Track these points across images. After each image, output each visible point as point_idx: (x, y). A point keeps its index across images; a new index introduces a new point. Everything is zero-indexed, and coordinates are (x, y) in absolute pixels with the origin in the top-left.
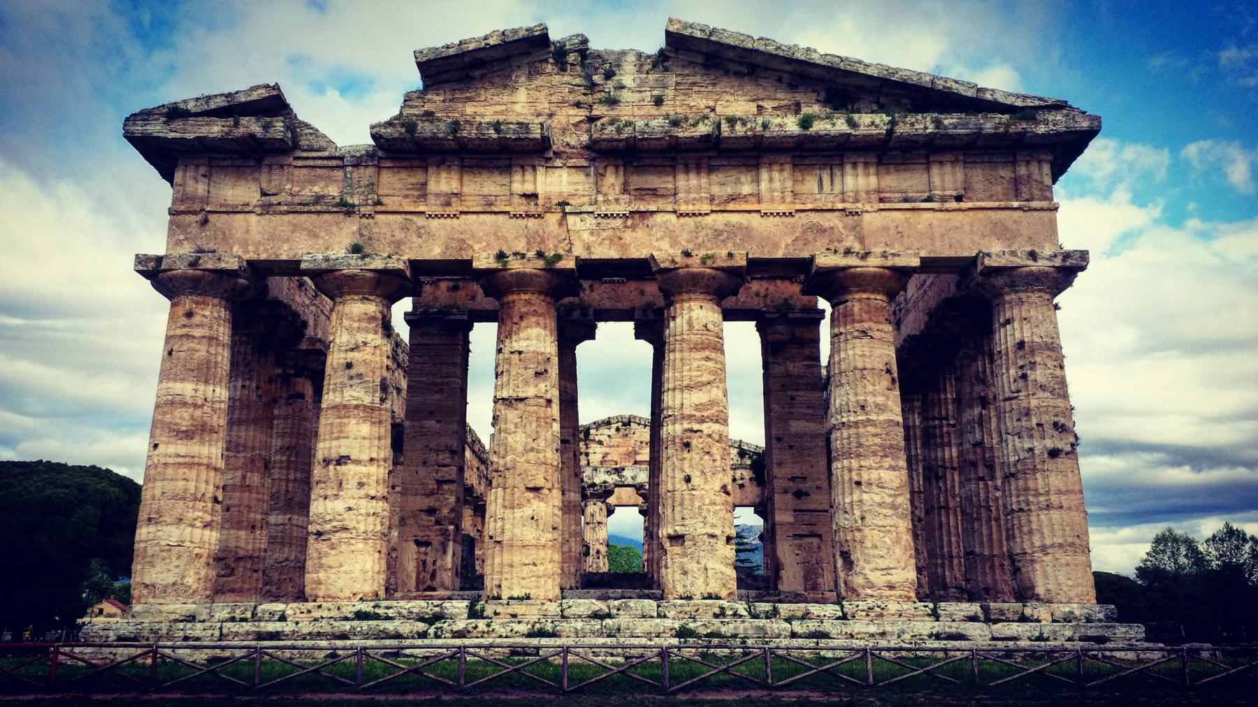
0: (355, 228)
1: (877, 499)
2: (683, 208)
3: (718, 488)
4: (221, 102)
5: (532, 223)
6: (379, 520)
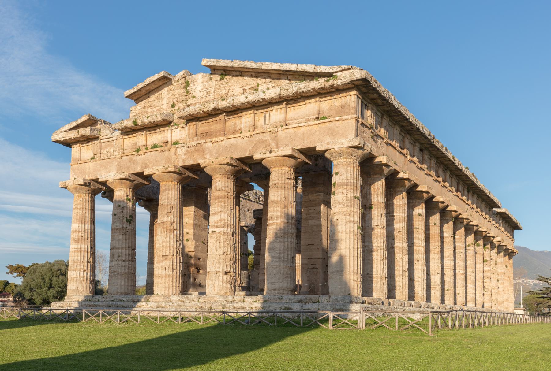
2: (214, 140)
6: (127, 268)
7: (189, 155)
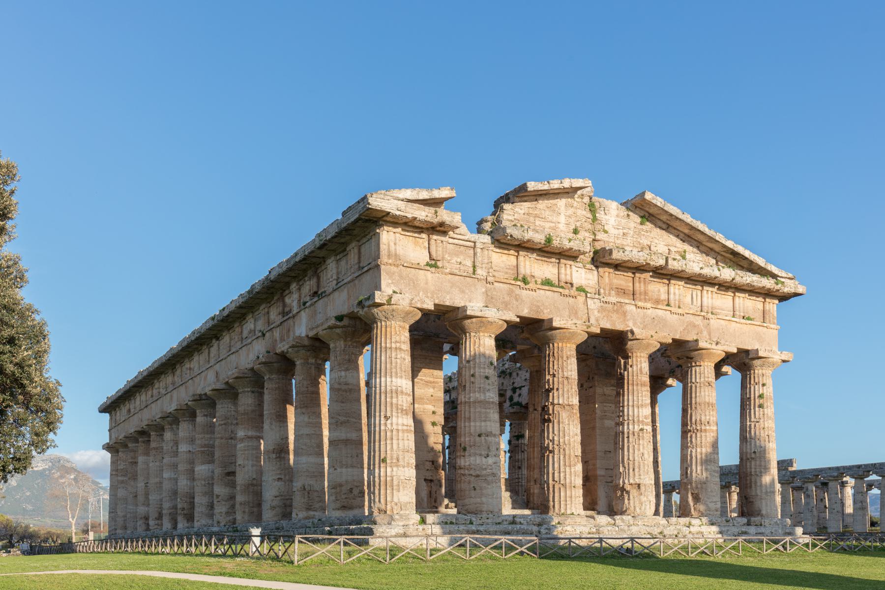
0: (484, 290)
2: (640, 304)
5: (571, 300)
7: (604, 314)
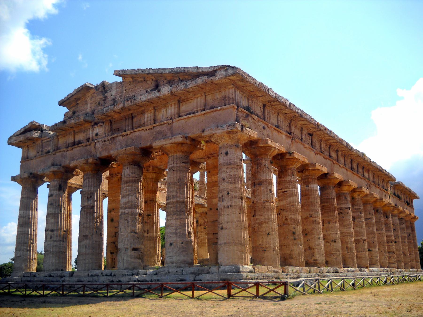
1: (171, 231)
3: (129, 231)
4: (23, 130)
